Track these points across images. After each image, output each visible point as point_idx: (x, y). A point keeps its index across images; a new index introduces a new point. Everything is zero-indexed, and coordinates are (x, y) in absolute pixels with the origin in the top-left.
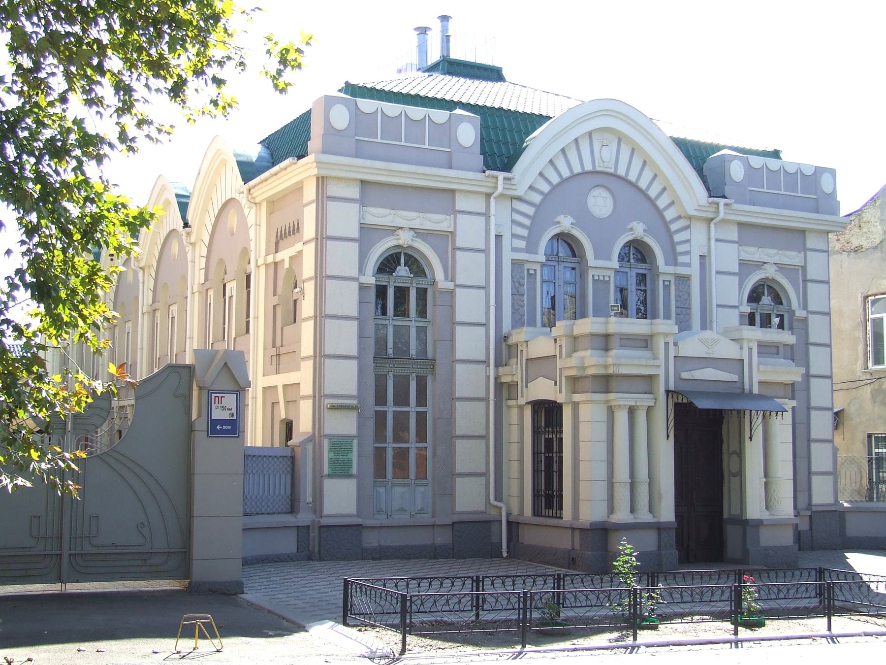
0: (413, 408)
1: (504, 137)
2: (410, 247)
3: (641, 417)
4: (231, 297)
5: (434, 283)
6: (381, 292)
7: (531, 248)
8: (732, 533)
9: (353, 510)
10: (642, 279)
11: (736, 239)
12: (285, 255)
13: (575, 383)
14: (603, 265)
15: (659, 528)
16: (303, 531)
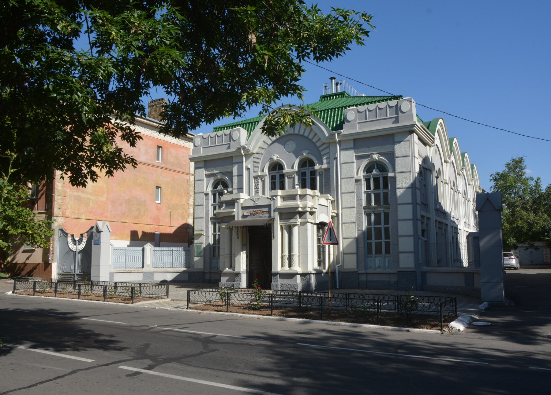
2: (221, 179)
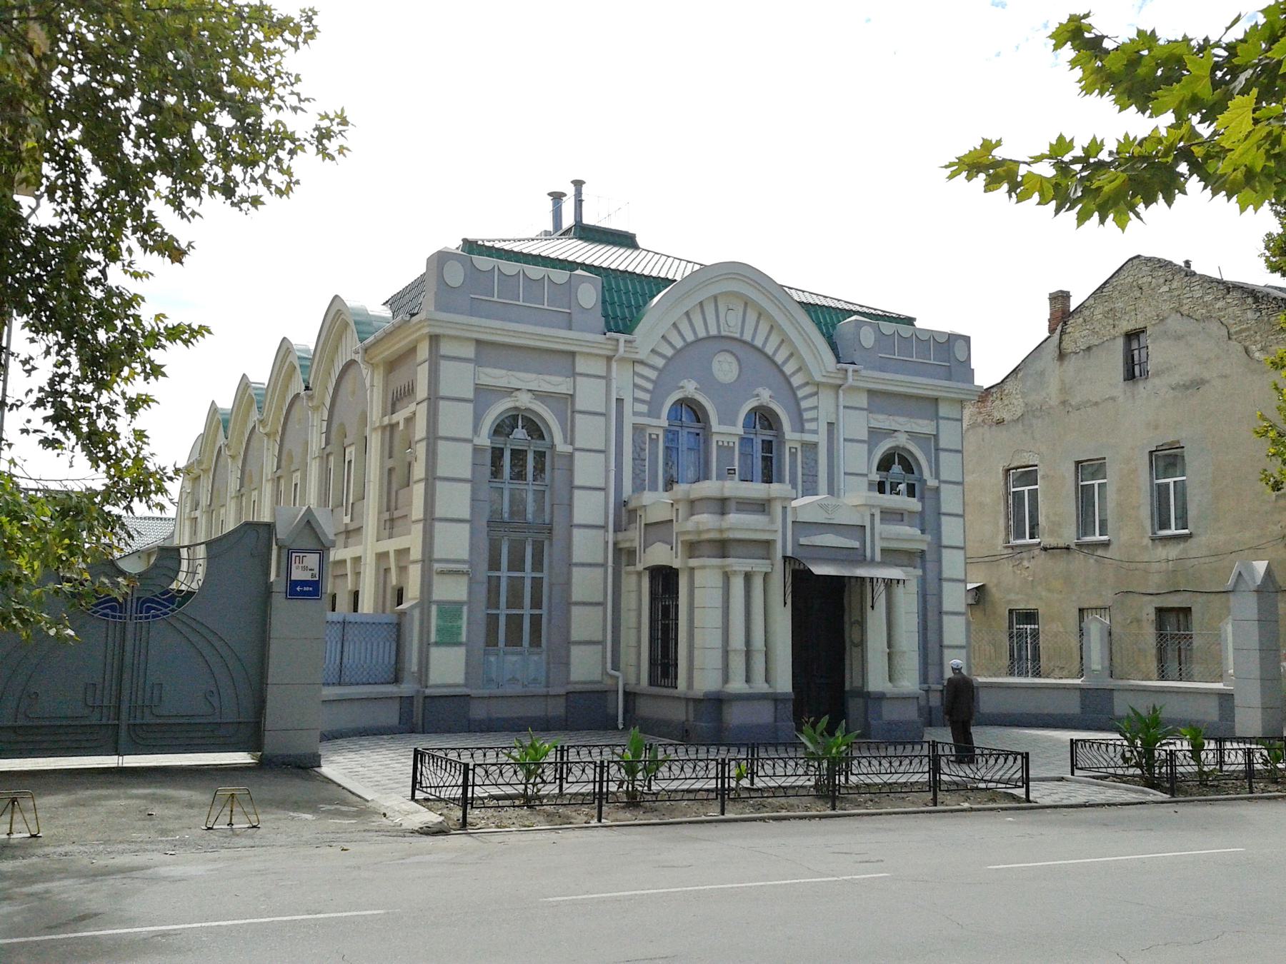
0: (528, 573)
1: (626, 298)
2: (528, 409)
3: (758, 583)
4: (350, 462)
5: (553, 446)
6: (497, 454)
7: (654, 413)
8: (854, 706)
9: (460, 679)
10: (767, 446)
11: (865, 404)
12: (400, 417)
13: (693, 548)
14: (727, 430)
15: (776, 699)
16: (406, 701)
